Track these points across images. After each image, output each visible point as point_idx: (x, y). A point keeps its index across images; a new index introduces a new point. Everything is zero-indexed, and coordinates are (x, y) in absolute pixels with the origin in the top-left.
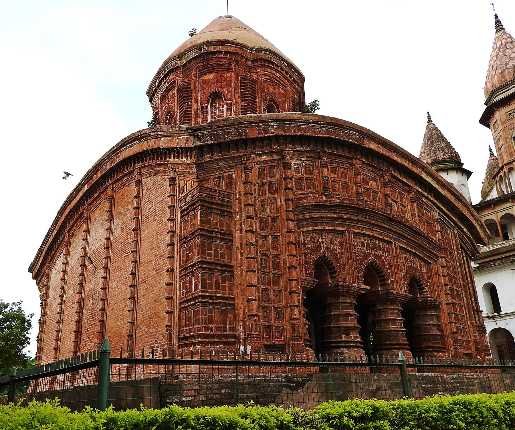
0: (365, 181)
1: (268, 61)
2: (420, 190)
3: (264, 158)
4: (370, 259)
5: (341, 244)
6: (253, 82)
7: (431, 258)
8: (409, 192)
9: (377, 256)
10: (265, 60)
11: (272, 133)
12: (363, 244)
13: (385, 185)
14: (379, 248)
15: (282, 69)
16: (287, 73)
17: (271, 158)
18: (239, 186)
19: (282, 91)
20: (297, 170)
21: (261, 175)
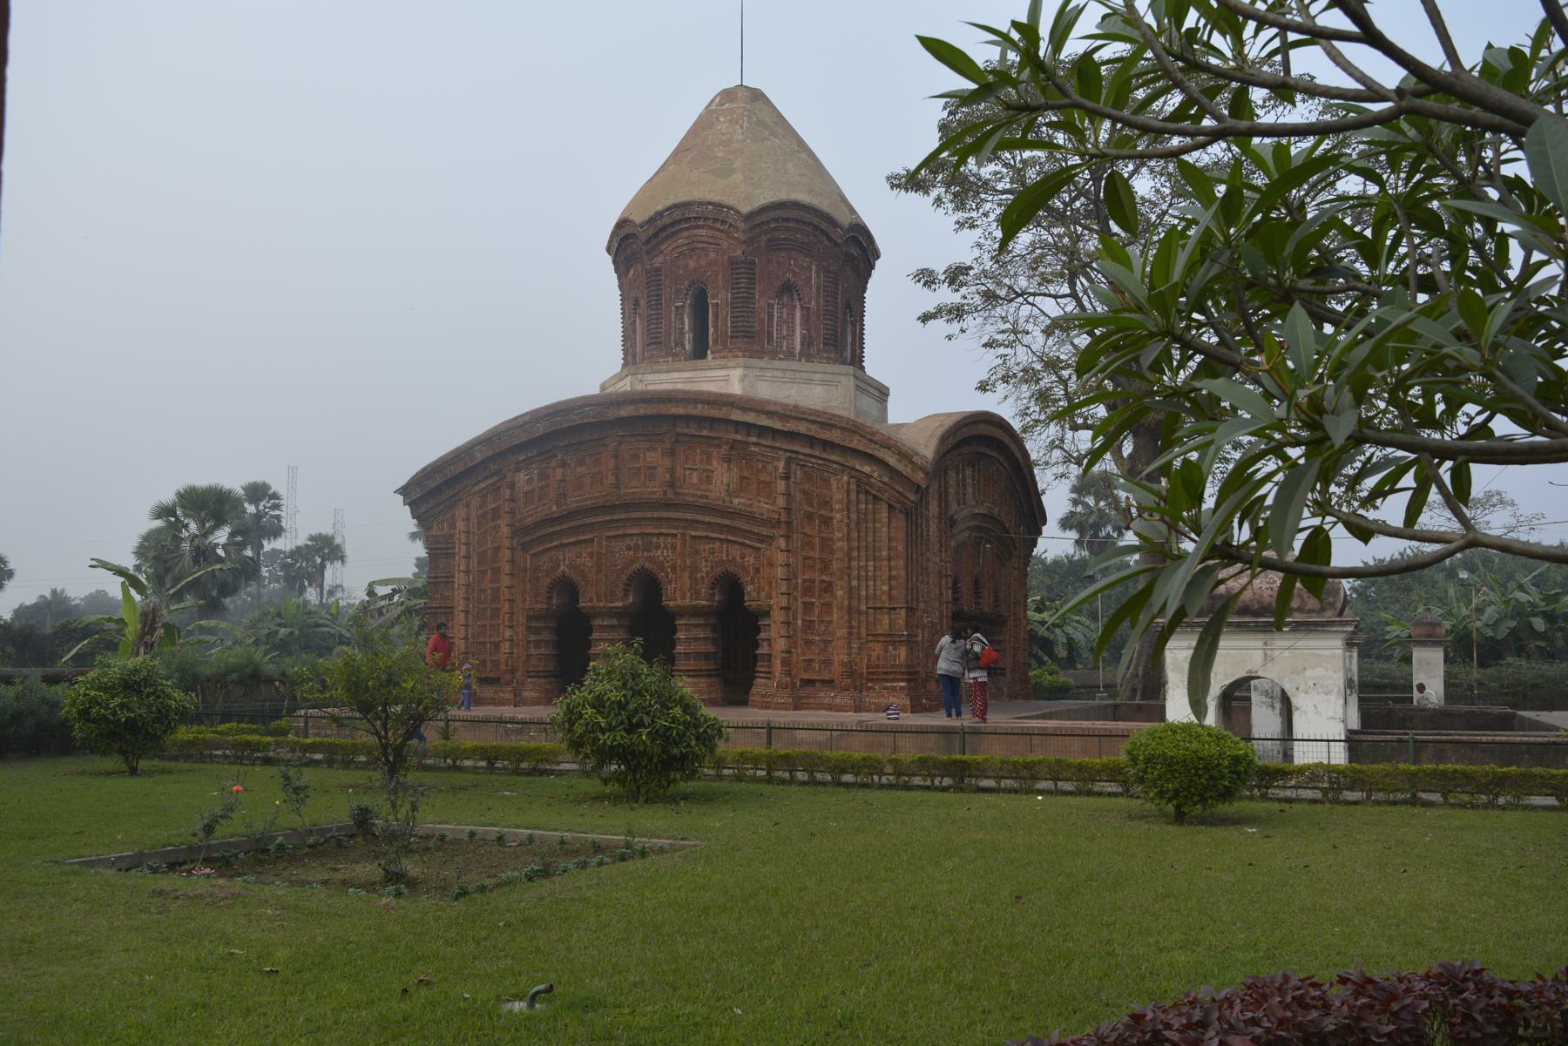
0: (636, 457)
1: (680, 221)
2: (739, 437)
3: (483, 485)
4: (637, 566)
5: (591, 555)
6: (658, 270)
7: (762, 541)
8: (719, 446)
9: (649, 559)
10: (672, 225)
11: (479, 457)
12: (629, 548)
13: (672, 453)
14: (658, 547)
15: (706, 219)
16: (715, 220)
17: (490, 481)
18: (460, 525)
19: (712, 255)
20: (530, 481)
21: (483, 504)
